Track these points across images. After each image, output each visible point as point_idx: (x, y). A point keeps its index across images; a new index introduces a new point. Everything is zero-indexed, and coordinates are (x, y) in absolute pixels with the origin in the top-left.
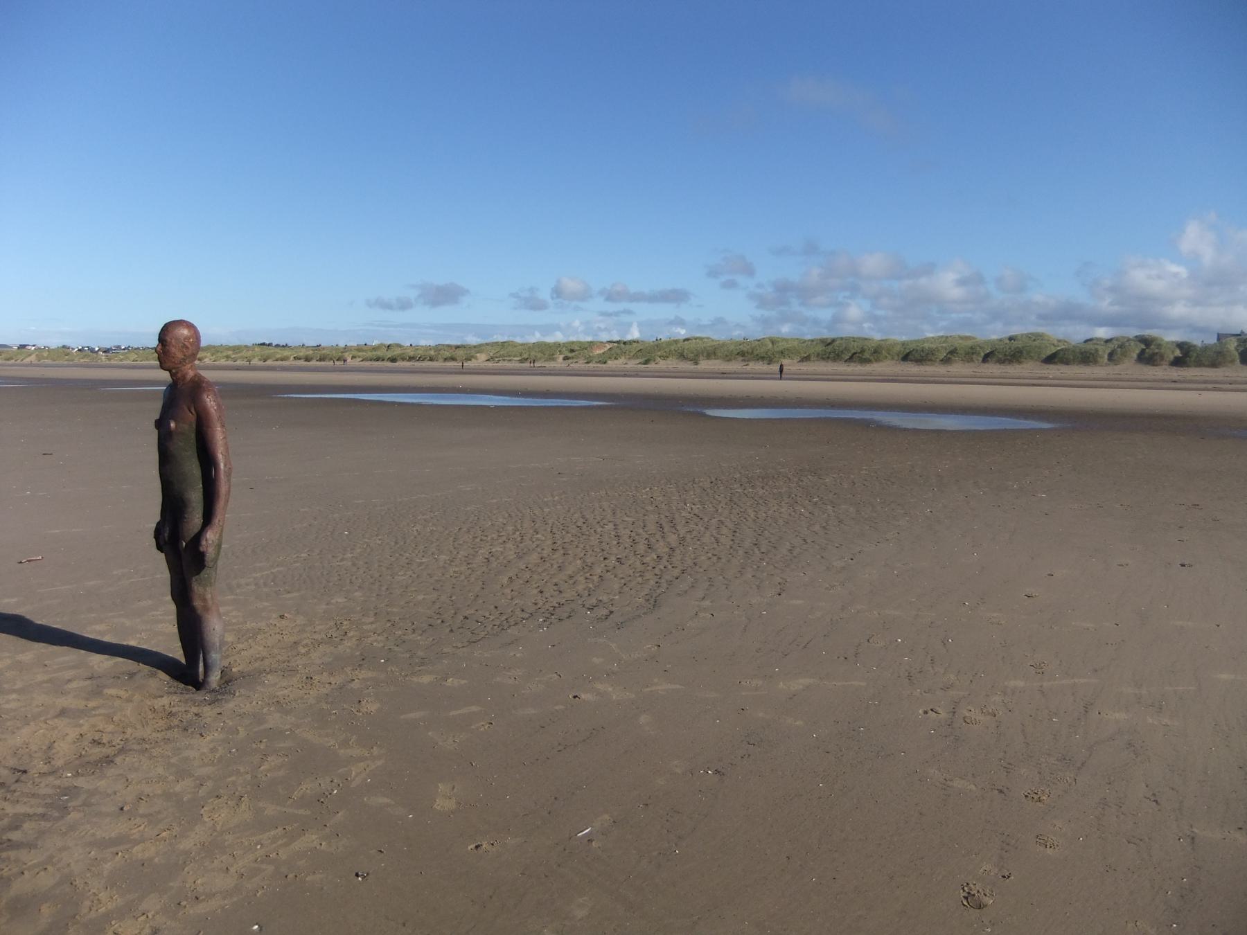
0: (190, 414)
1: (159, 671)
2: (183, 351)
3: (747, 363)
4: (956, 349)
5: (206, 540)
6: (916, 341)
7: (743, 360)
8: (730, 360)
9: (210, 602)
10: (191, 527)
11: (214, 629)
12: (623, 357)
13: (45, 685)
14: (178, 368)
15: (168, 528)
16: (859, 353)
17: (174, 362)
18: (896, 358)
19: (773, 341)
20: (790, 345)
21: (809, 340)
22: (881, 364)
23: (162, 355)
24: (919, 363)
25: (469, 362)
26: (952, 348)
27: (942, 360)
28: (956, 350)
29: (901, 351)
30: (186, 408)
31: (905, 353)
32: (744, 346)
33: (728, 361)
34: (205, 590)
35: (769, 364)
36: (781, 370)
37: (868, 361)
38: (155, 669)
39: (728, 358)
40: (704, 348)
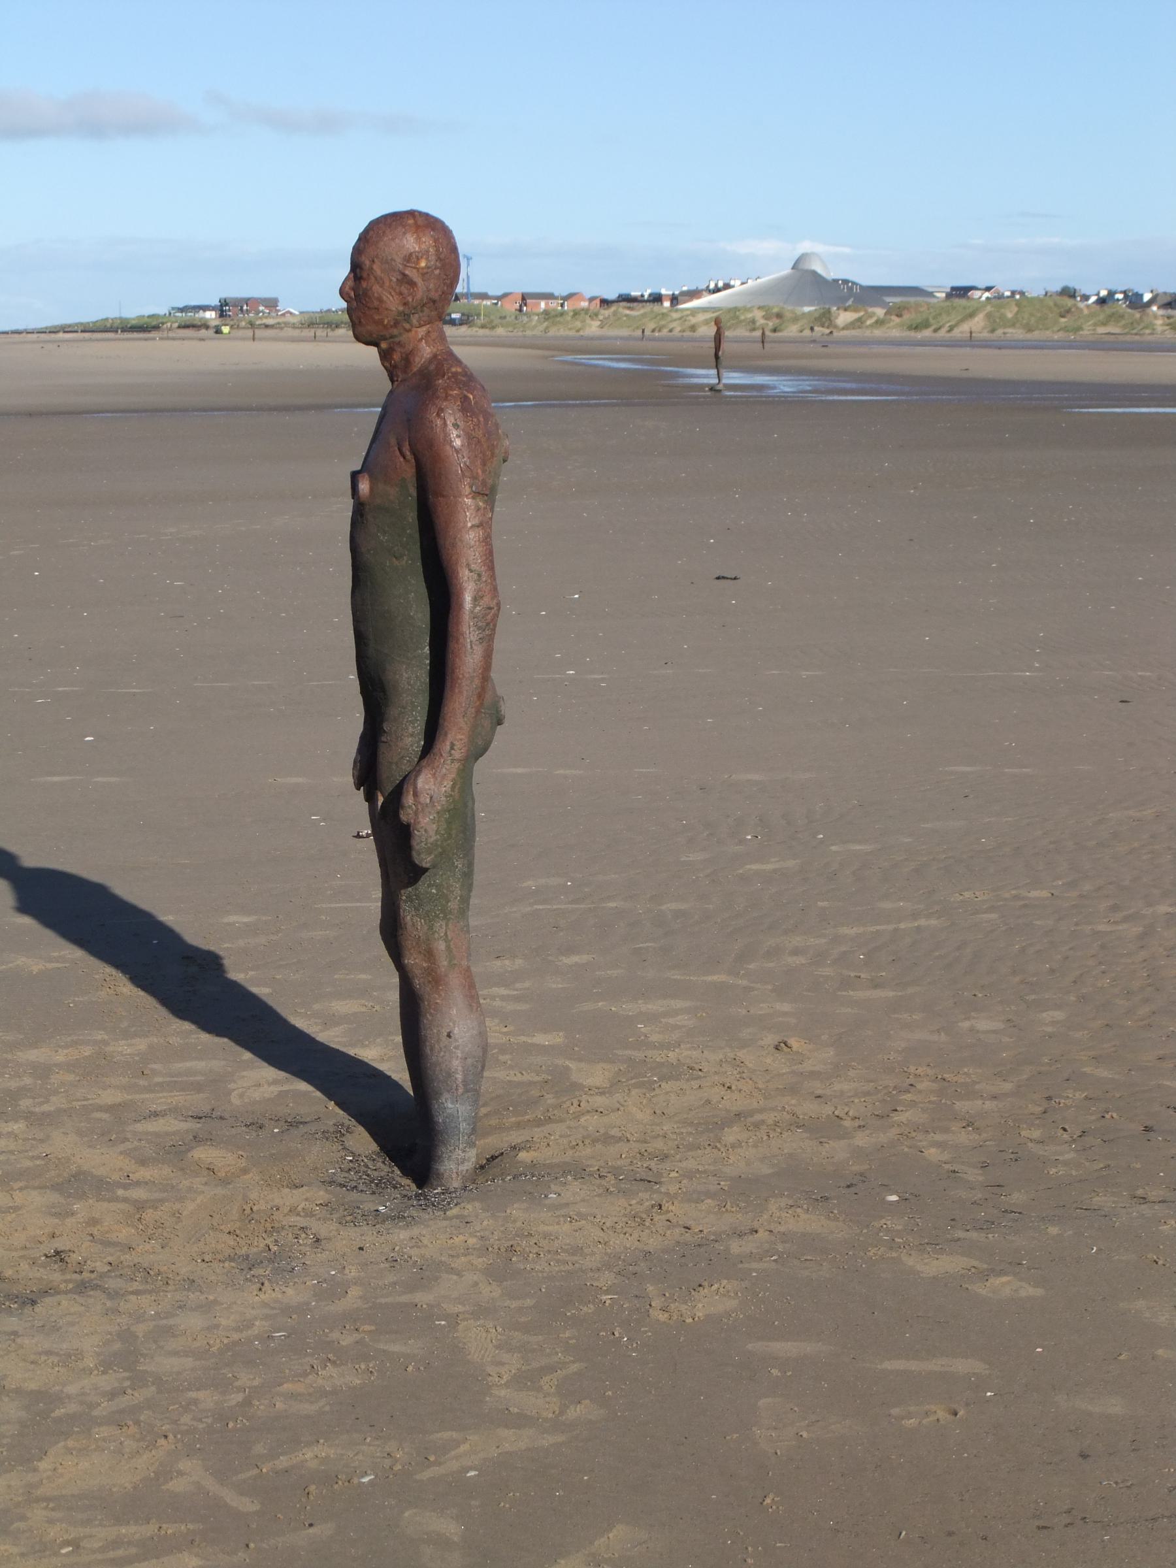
0: (402, 459)
1: (361, 1129)
2: (401, 294)
5: (416, 795)
9: (443, 963)
11: (449, 1036)
13: (98, 1115)
14: (392, 337)
17: (381, 322)
30: (393, 441)
34: (431, 928)
38: (353, 1122)
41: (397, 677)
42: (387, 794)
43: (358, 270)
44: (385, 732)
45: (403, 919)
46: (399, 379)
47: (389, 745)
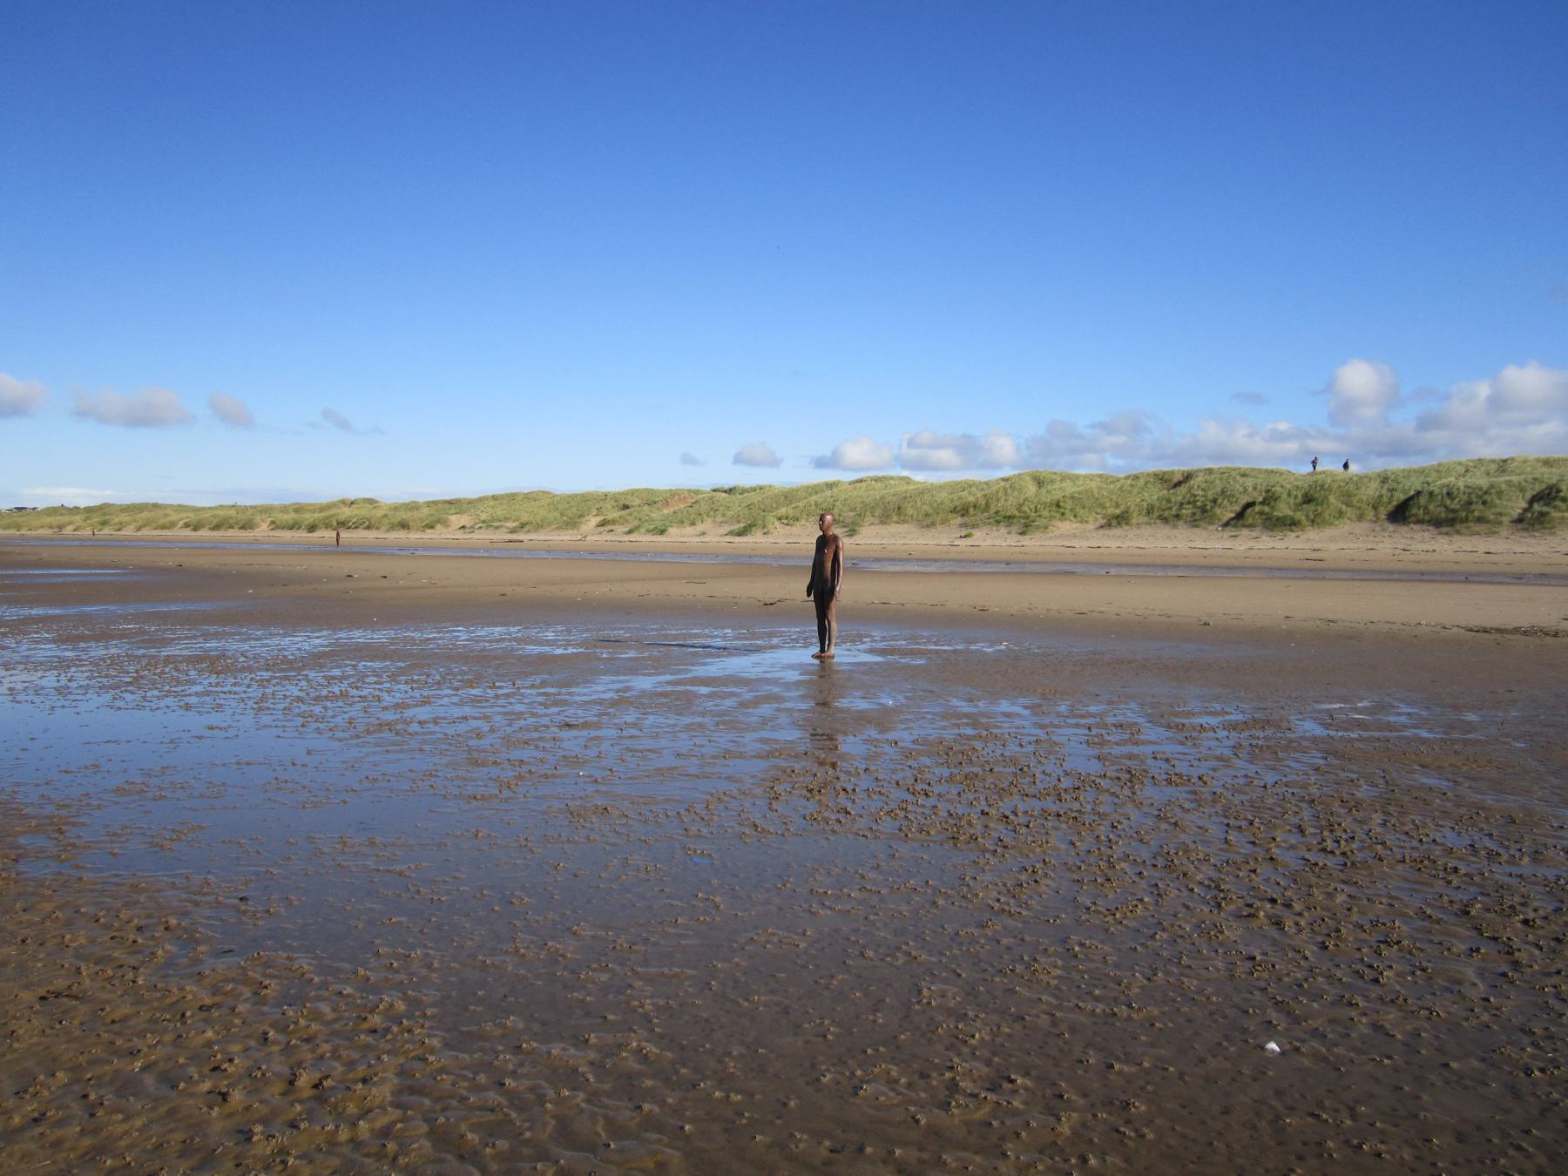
3: (969, 531)
4: (1551, 488)
6: (1422, 472)
7: (961, 525)
8: (933, 524)
12: (710, 520)
16: (1262, 503)
18: (1370, 514)
19: (1040, 482)
20: (1082, 488)
21: (1127, 478)
22: (1328, 532)
24: (1445, 529)
25: (430, 531)
26: (1538, 488)
27: (1520, 520)
28: (1559, 491)
29: (1381, 496)
31: (1395, 503)
32: (970, 493)
33: (928, 526)
35: (1023, 533)
36: (822, 589)
37: (1292, 524)
39: (928, 521)
40: (882, 498)
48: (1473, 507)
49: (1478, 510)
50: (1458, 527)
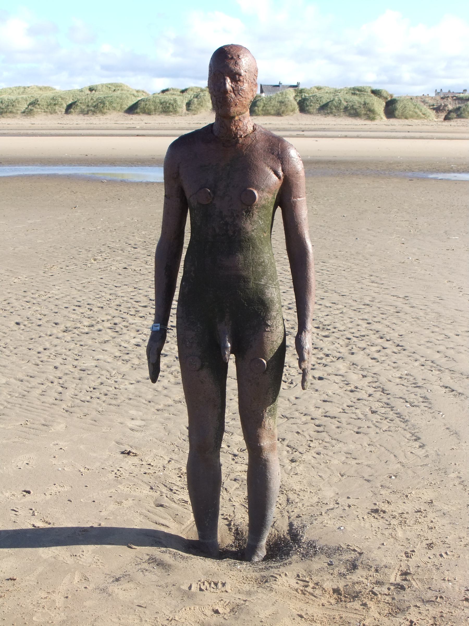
4: (37, 100)
10: (275, 339)
15: (229, 345)
23: (233, 95)
26: (32, 100)
27: (24, 112)
28: (38, 101)
41: (273, 295)
42: (269, 359)
43: (237, 76)
44: (269, 326)
45: (264, 422)
46: (243, 136)
47: (272, 332)
48: (9, 107)
49: (10, 108)
50: (3, 115)
